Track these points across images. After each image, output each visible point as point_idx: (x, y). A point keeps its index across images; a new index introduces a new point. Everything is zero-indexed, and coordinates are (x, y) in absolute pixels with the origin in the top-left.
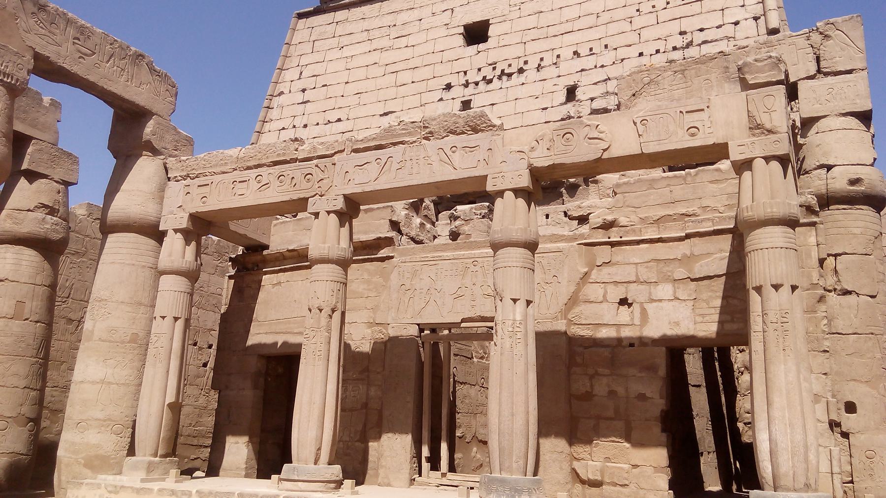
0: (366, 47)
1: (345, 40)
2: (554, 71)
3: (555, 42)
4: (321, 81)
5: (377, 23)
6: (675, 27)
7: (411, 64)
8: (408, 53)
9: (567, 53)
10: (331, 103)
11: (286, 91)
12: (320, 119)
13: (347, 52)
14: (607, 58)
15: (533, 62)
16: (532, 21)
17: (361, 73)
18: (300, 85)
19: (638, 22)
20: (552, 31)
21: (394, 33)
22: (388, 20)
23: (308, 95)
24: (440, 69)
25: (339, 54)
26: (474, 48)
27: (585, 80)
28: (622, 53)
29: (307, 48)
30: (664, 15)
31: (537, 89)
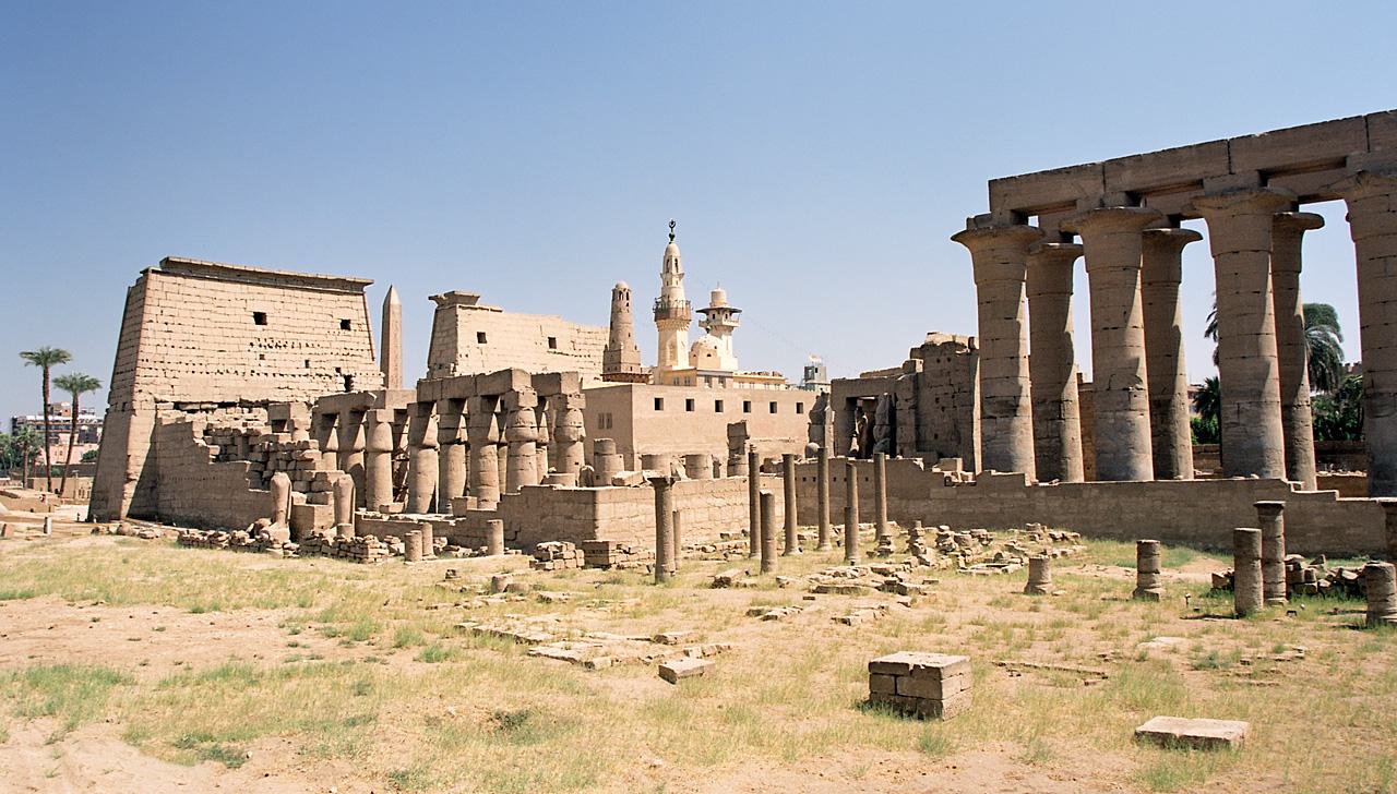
0: (201, 307)
1: (186, 298)
2: (297, 350)
3: (297, 336)
4: (177, 321)
5: (204, 293)
6: (343, 345)
7: (229, 325)
8: (226, 318)
9: (303, 345)
10: (186, 337)
11: (154, 320)
12: (181, 344)
13: (189, 306)
14: (319, 351)
15: (289, 345)
16: (286, 321)
17: (202, 323)
18: (162, 319)
19: (331, 338)
20: (296, 330)
21: (217, 303)
22: (211, 294)
23: (170, 327)
24: (247, 334)
25: (185, 306)
26: (260, 327)
27: (313, 359)
28: (325, 350)
29: (163, 296)
30: (339, 338)
31: (293, 357)
